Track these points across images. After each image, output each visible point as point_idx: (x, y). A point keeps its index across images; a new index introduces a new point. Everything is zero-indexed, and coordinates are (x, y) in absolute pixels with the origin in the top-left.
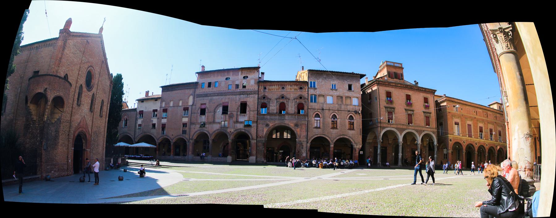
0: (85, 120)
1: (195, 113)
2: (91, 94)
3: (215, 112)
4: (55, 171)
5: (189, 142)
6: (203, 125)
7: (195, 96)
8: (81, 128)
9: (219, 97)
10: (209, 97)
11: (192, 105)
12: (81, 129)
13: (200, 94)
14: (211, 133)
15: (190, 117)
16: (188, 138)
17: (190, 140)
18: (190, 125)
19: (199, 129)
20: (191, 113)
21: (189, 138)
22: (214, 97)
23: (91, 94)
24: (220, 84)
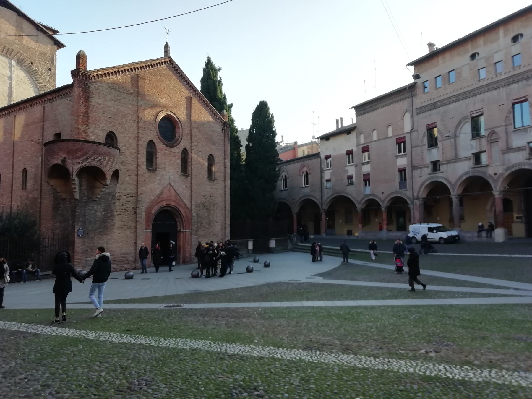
0: (172, 190)
1: (417, 146)
2: (178, 150)
3: (455, 137)
5: (412, 203)
6: (436, 166)
7: (414, 110)
9: (461, 102)
10: (441, 108)
11: (410, 132)
12: (164, 203)
13: (423, 105)
14: (453, 181)
15: (410, 155)
16: (411, 197)
17: (414, 200)
18: (412, 170)
19: (429, 176)
20: (410, 147)
21: (413, 195)
22: (451, 106)
23: (177, 151)
24: (459, 75)
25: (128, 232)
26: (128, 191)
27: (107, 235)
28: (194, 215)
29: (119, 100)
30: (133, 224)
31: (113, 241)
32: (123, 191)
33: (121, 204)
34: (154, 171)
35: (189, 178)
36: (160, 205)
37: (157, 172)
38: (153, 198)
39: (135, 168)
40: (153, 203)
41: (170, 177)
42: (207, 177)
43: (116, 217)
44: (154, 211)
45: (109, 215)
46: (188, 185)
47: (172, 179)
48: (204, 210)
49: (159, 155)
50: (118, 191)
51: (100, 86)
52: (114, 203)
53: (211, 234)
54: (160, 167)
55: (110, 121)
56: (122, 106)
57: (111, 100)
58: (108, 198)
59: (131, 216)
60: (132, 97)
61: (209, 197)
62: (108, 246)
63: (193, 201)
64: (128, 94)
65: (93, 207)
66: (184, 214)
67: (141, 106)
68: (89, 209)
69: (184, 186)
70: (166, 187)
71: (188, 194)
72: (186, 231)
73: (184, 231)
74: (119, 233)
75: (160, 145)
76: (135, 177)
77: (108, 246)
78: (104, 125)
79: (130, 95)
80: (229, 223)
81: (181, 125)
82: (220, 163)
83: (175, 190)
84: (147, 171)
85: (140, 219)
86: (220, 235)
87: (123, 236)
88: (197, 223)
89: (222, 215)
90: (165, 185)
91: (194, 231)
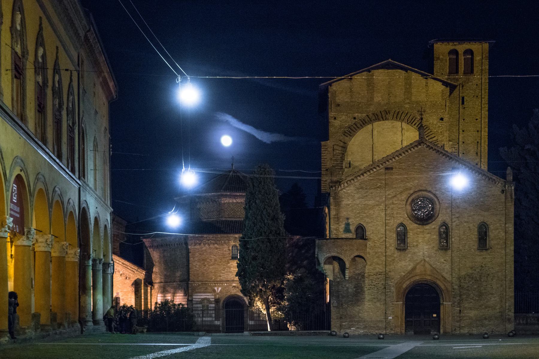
0: (427, 265)
4: (358, 328)
8: (418, 276)
12: (417, 278)
25: (378, 304)
26: (377, 270)
27: (358, 306)
28: (456, 287)
29: (367, 196)
30: (383, 298)
31: (364, 311)
32: (372, 271)
33: (370, 281)
34: (404, 250)
35: (449, 252)
36: (412, 280)
37: (408, 250)
38: (403, 274)
39: (383, 250)
40: (403, 278)
41: (424, 253)
42: (476, 247)
43: (366, 292)
44: (404, 286)
45: (360, 291)
46: (448, 258)
47: (426, 255)
48: (471, 282)
49: (410, 235)
50: (367, 271)
51: (349, 190)
52: (364, 281)
53: (483, 307)
54: (411, 246)
55: (358, 215)
56: (370, 200)
57: (359, 198)
58: (358, 278)
59: (380, 290)
60: (379, 190)
61: (480, 268)
62: (360, 315)
63: (454, 274)
64: (374, 188)
65: (345, 285)
66: (443, 287)
67: (389, 195)
68: (342, 287)
69: (442, 260)
70: (418, 264)
71: (448, 267)
72: (446, 303)
73: (444, 303)
74: (370, 305)
75: (411, 226)
76: (384, 258)
77: (360, 315)
78: (353, 220)
79: (378, 189)
80: (513, 294)
81: (438, 200)
82: (497, 229)
83: (430, 265)
84: (396, 251)
85: (389, 293)
86: (497, 307)
87: (373, 307)
88: (460, 296)
89: (502, 285)
90: (418, 262)
91: (456, 304)
